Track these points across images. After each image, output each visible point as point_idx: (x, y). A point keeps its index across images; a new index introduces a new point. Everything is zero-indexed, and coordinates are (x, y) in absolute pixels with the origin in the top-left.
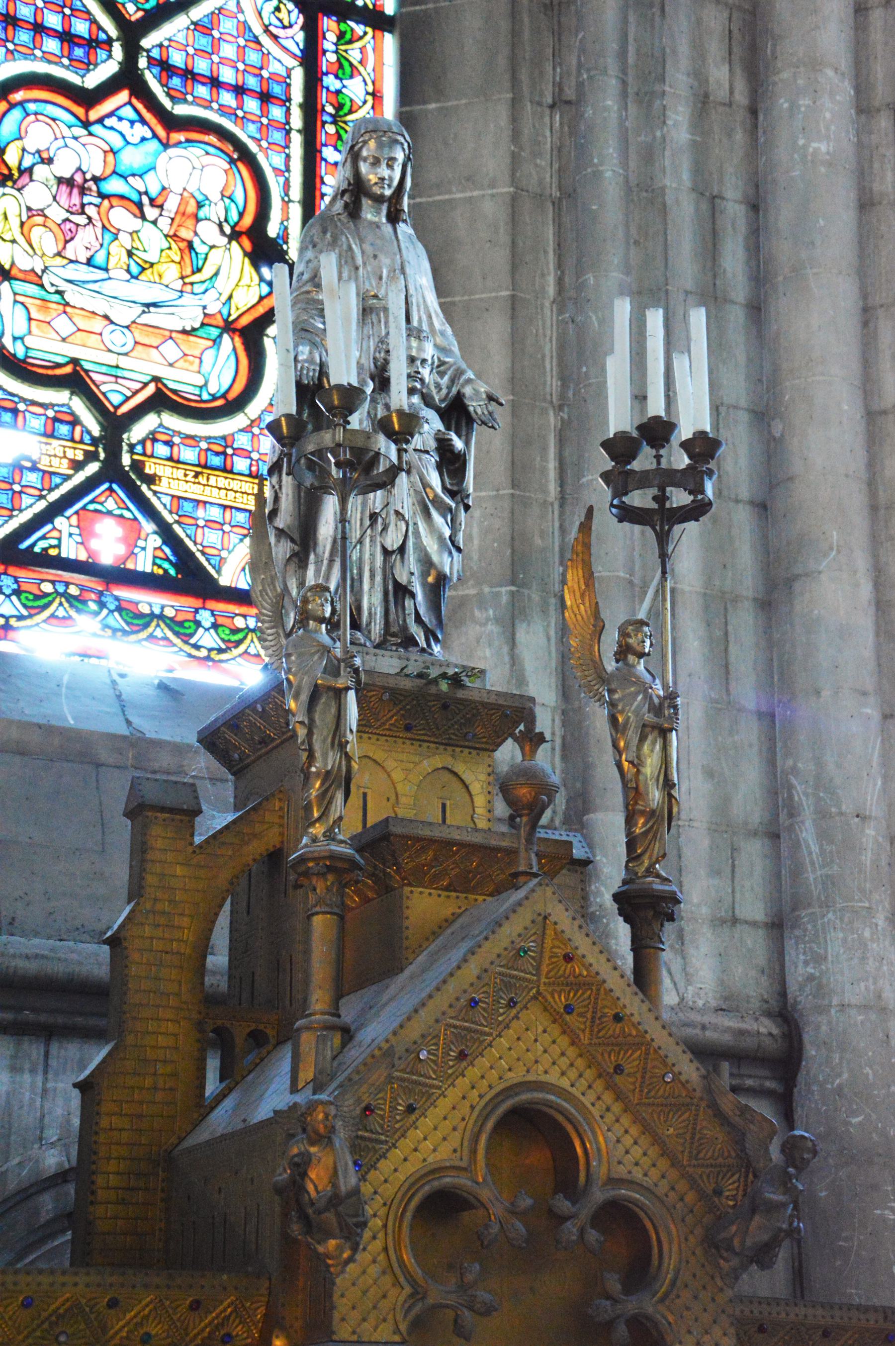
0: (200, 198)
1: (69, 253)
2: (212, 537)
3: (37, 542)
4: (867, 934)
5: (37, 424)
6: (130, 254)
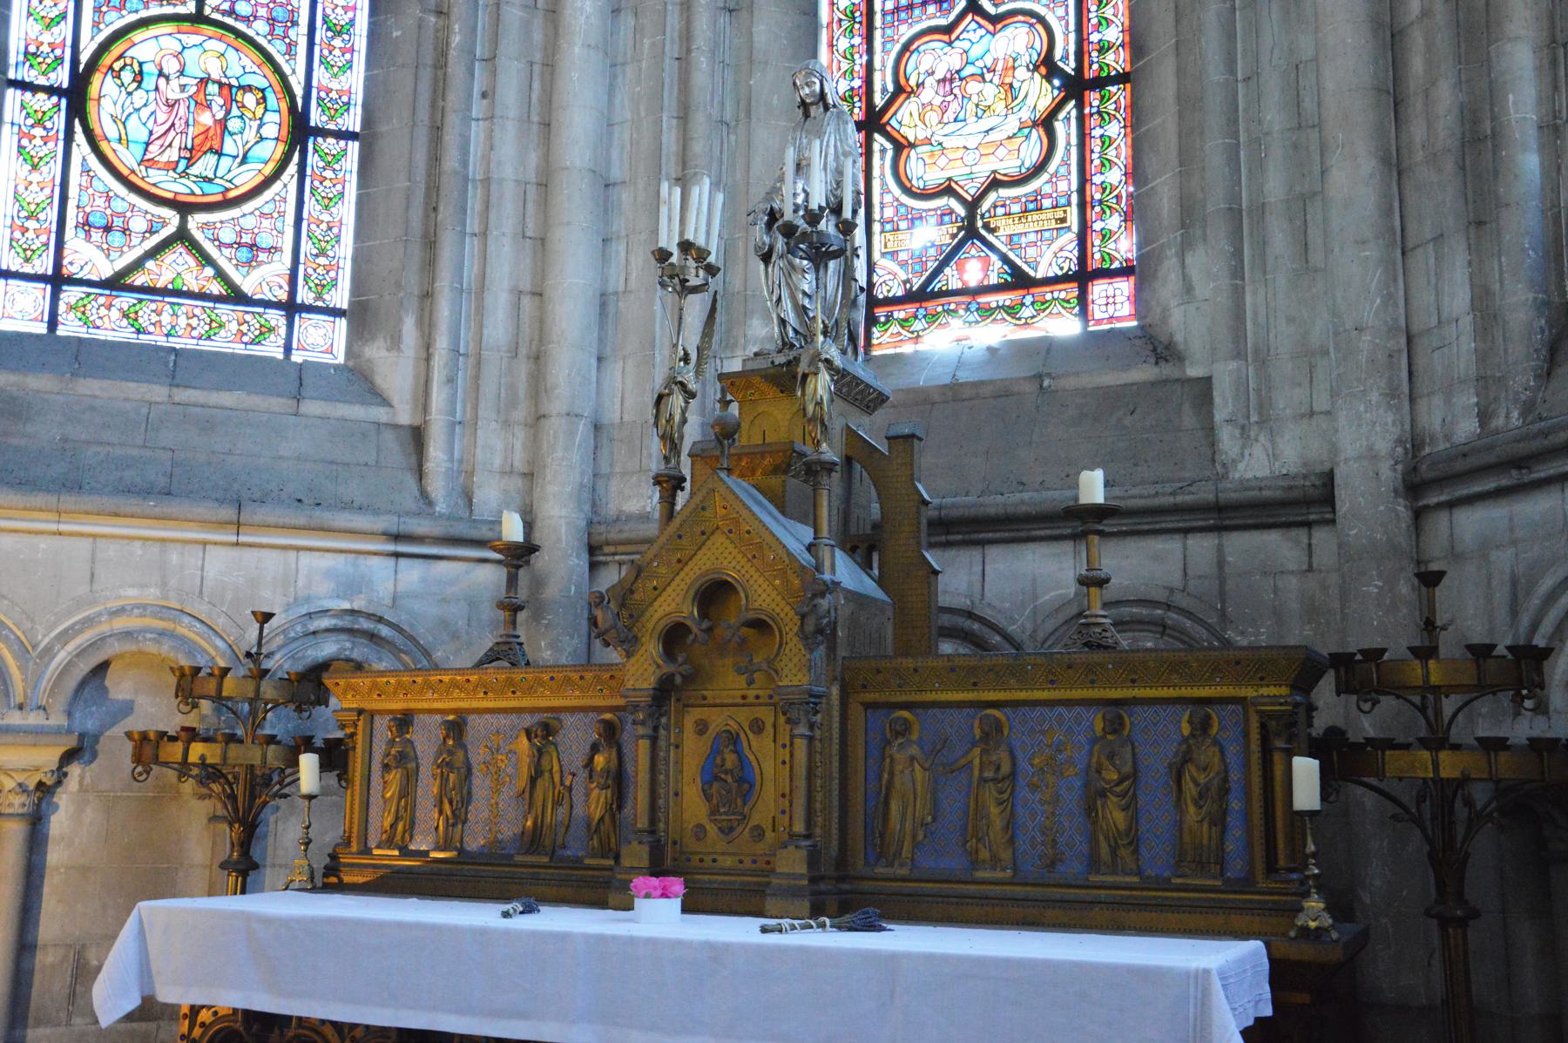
0: (1014, 55)
1: (945, 120)
2: (1031, 252)
3: (937, 285)
4: (1362, 408)
5: (933, 220)
6: (977, 106)
